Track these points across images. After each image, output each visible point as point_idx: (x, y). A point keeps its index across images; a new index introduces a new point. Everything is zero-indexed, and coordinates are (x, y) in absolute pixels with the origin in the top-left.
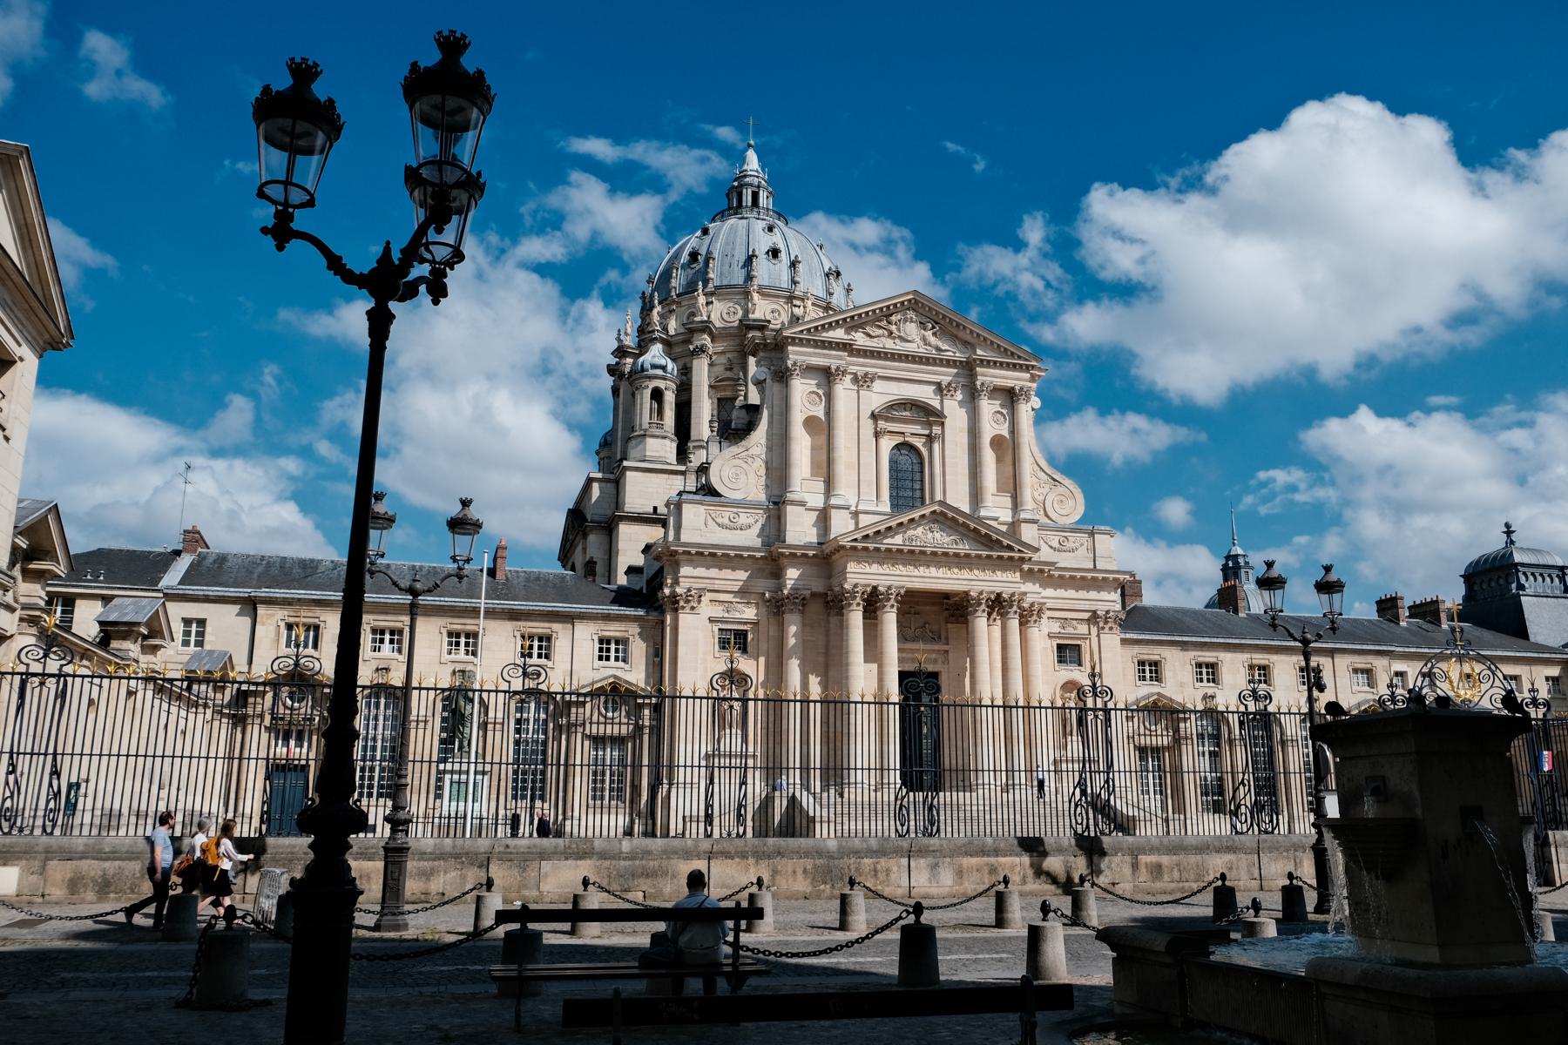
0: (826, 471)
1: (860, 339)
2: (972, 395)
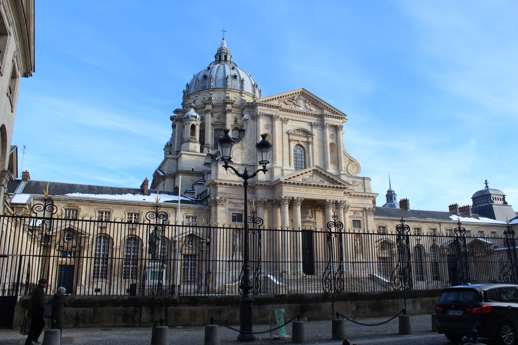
1: (284, 106)
2: (323, 126)
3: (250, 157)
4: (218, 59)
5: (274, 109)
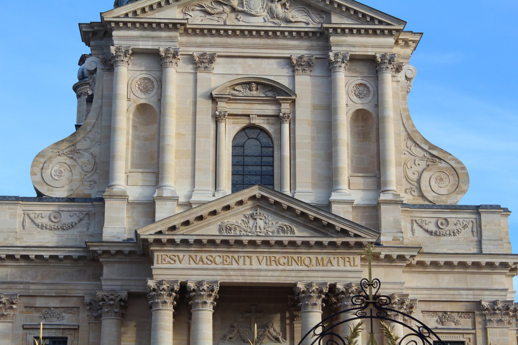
1: (196, 19)
3: (95, 177)
5: (164, 34)
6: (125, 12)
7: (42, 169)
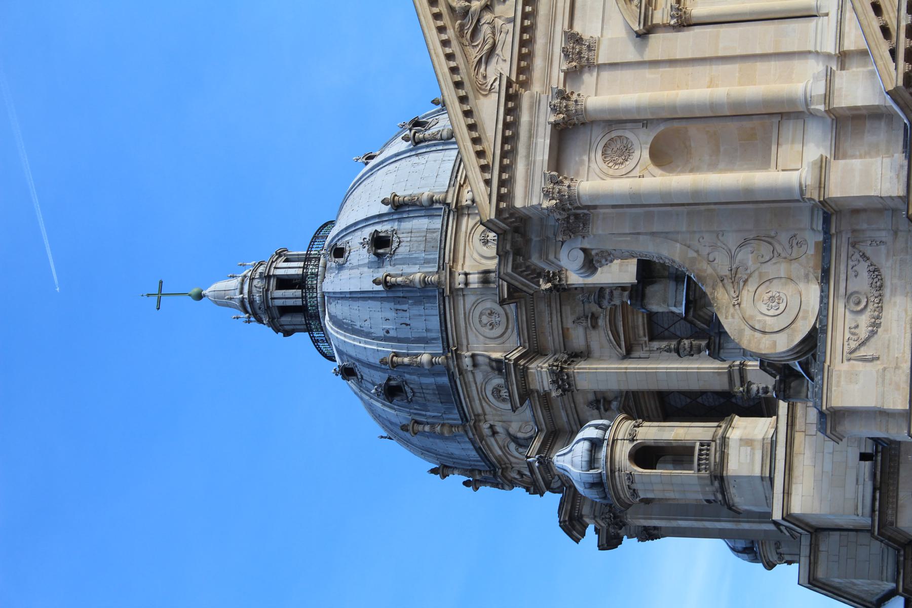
0: (761, 124)
1: (502, 67)
3: (784, 237)
4: (299, 319)
5: (525, 118)
6: (482, 184)
7: (764, 332)
